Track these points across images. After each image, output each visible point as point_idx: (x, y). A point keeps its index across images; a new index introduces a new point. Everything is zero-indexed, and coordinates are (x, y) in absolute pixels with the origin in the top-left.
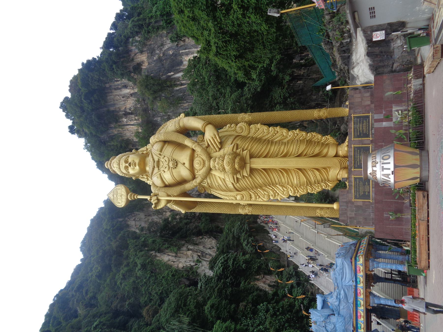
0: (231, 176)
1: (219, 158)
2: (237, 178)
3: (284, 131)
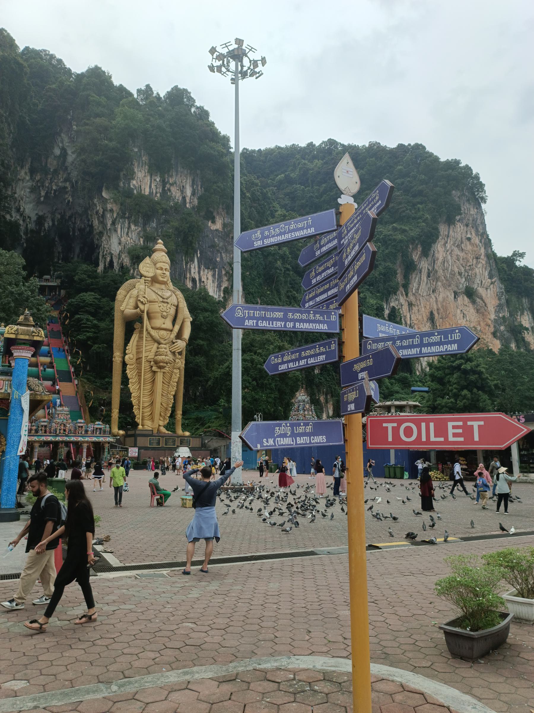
0: (153, 357)
1: (167, 352)
2: (151, 361)
3: (173, 393)
